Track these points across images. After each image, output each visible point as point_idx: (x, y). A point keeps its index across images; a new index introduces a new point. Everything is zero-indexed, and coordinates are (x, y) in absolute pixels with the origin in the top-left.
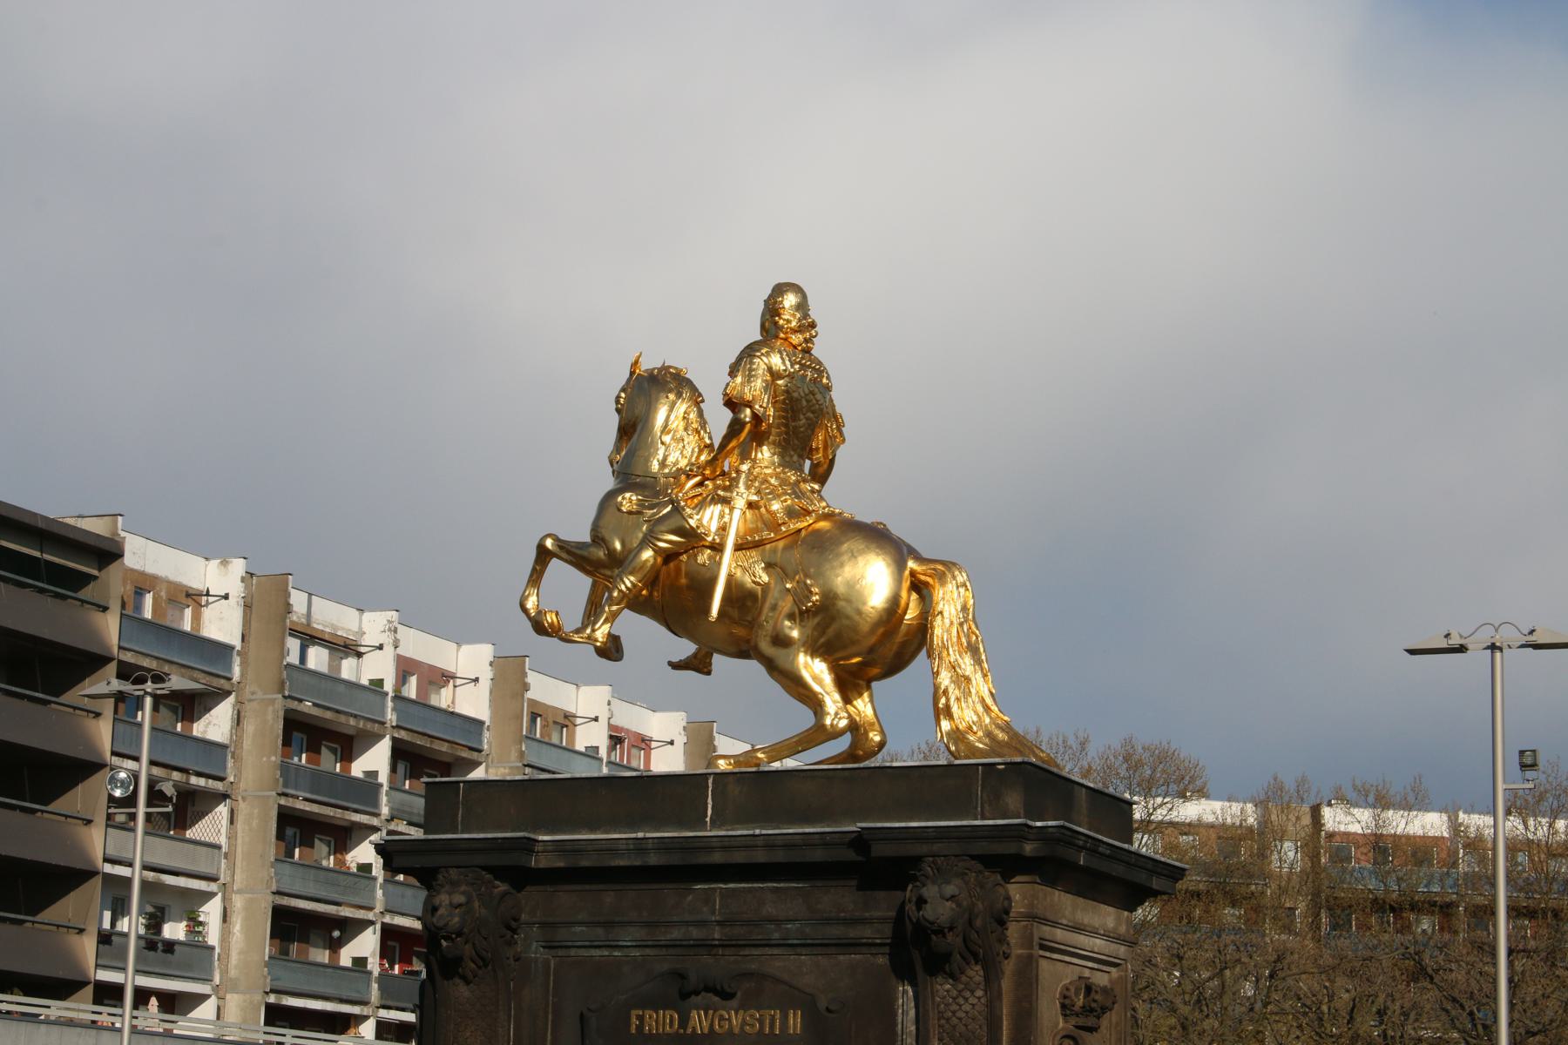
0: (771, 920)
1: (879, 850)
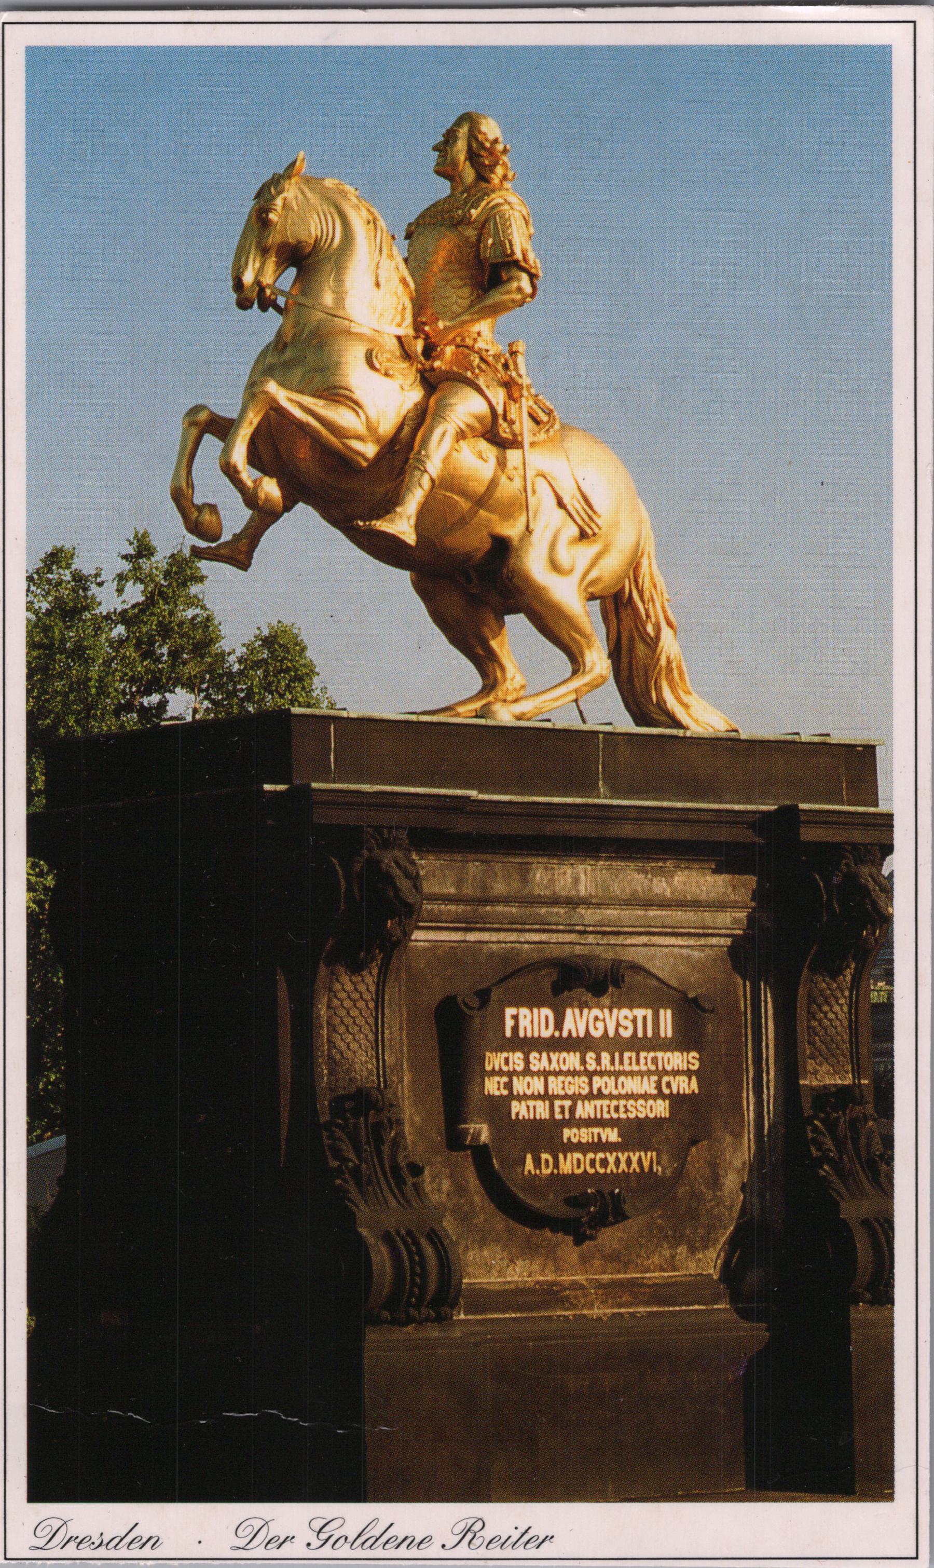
1: (808, 834)
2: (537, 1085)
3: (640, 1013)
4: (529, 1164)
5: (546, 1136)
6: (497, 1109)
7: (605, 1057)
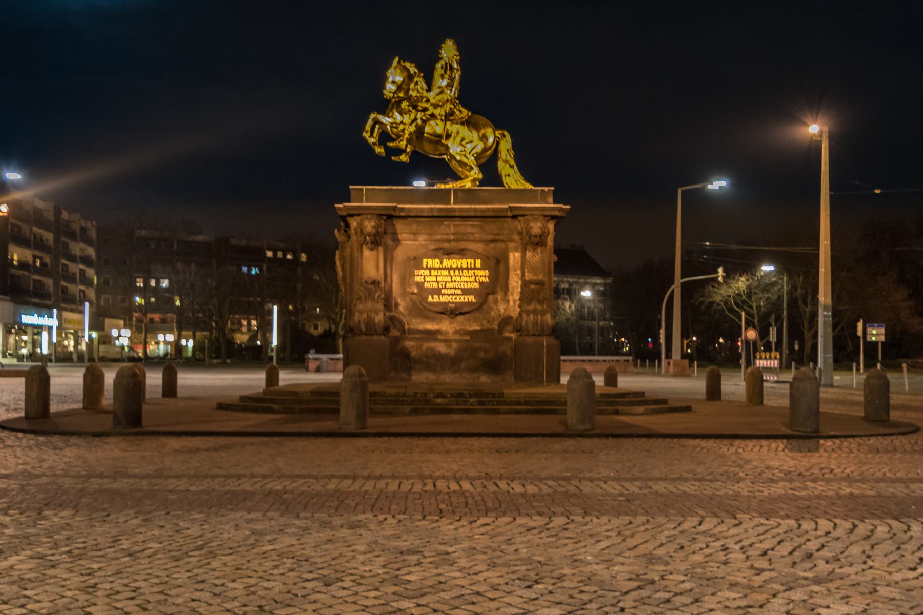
0: (470, 233)
2: (434, 279)
3: (469, 261)
4: (430, 297)
5: (438, 292)
6: (420, 285)
7: (457, 272)
